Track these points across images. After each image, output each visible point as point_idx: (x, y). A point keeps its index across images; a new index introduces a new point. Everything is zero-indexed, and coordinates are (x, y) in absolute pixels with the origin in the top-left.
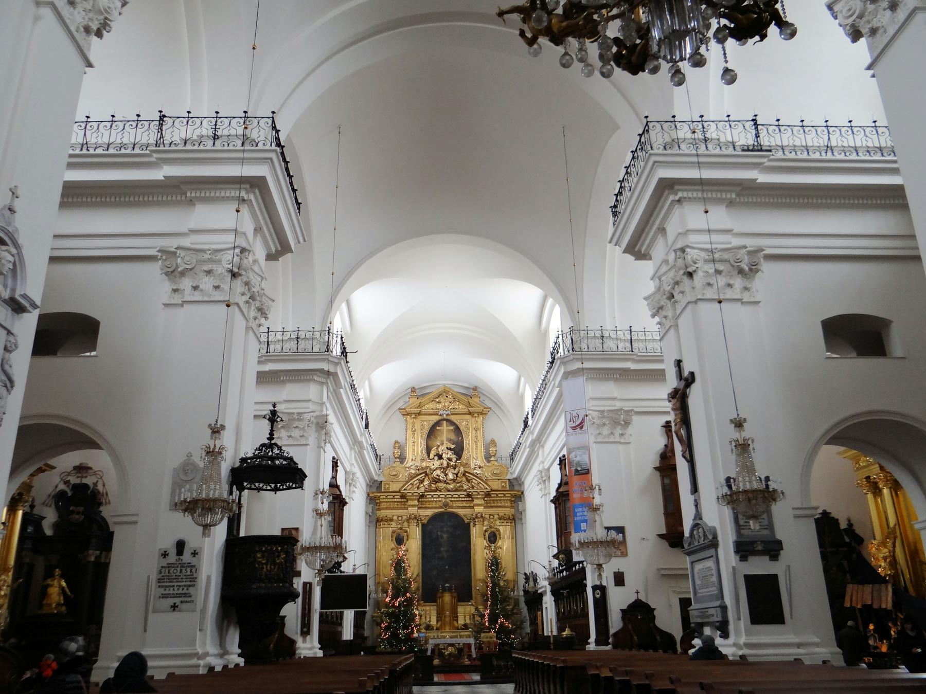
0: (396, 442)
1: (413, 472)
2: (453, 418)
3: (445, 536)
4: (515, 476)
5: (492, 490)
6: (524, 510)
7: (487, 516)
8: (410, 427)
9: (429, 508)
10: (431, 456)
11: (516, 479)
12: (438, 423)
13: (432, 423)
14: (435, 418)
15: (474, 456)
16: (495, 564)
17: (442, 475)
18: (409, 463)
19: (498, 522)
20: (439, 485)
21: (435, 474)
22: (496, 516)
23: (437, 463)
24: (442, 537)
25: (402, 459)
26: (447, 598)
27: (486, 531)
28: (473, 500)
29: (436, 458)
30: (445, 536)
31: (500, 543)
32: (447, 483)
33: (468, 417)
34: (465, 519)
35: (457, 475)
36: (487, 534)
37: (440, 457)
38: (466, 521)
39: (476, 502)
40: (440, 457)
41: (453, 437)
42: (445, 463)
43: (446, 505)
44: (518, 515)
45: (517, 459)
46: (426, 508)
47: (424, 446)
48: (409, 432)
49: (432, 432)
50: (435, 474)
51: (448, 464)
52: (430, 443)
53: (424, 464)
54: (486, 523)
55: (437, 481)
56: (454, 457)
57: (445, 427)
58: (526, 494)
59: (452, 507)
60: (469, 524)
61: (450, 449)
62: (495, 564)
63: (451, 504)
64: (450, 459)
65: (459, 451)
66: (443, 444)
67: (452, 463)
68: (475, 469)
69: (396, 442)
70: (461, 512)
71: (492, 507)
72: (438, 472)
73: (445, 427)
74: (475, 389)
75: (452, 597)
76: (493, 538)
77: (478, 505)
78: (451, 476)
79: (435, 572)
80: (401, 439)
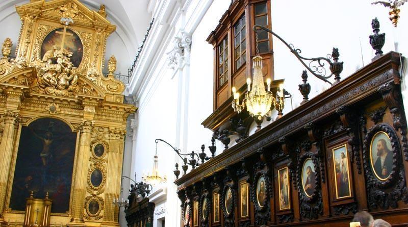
0: (8, 40)
1: (20, 67)
2: (76, 30)
3: (47, 142)
4: (131, 92)
5: (106, 102)
6: (136, 128)
7: (97, 128)
8: (27, 28)
9: (33, 111)
10: (44, 59)
11: (131, 97)
12: (59, 30)
13: (52, 29)
14: (58, 26)
15: (91, 67)
16: (97, 179)
17: (53, 78)
18: (19, 60)
19: (107, 136)
20: (49, 89)
21: (45, 77)
22: (106, 130)
23: (49, 66)
24: (44, 141)
25: (11, 56)
26: (37, 205)
27: (93, 143)
28: (83, 110)
29: (50, 61)
30: (47, 142)
31: (106, 156)
32: (58, 89)
33: (90, 31)
34: (71, 126)
35: (70, 81)
36: (94, 146)
37: (54, 61)
38: (73, 130)
39: (87, 109)
40: (54, 61)
41: (72, 46)
42: (58, 67)
43: (53, 110)
44: (128, 133)
45: (134, 74)
46: (29, 110)
47: (38, 49)
48: (25, 33)
49: (50, 38)
50: (45, 77)
51: (62, 70)
52: (46, 47)
53: (36, 64)
54: (95, 134)
55: (47, 84)
56: (70, 65)
57: (64, 32)
58: (141, 111)
59: (60, 114)
60: (76, 134)
61: (67, 56)
62: (97, 179)
63: (58, 110)
64: (66, 66)
65: (76, 60)
66: (61, 49)
67: (66, 69)
68: (90, 76)
69: (8, 40)
70: (68, 120)
71: (102, 120)
72: (50, 75)
73: (64, 32)
74: (103, 7)
75: (45, 205)
76: (99, 150)
77: (89, 113)
78: (62, 82)
79: (29, 178)
80: (14, 41)
